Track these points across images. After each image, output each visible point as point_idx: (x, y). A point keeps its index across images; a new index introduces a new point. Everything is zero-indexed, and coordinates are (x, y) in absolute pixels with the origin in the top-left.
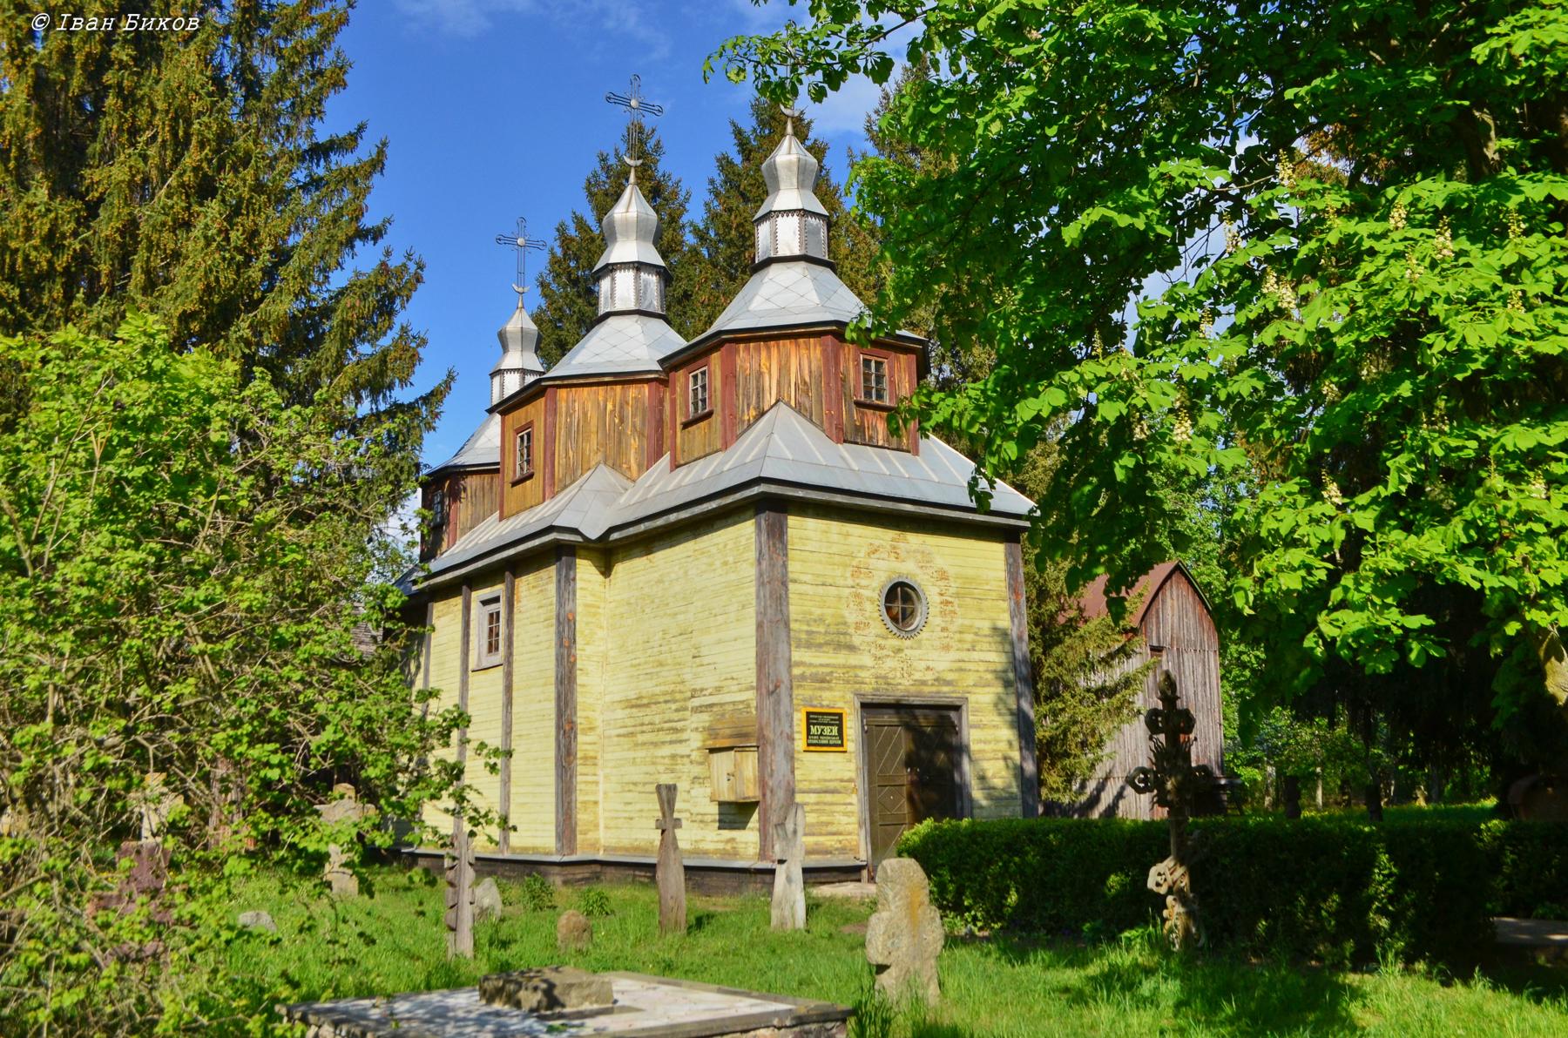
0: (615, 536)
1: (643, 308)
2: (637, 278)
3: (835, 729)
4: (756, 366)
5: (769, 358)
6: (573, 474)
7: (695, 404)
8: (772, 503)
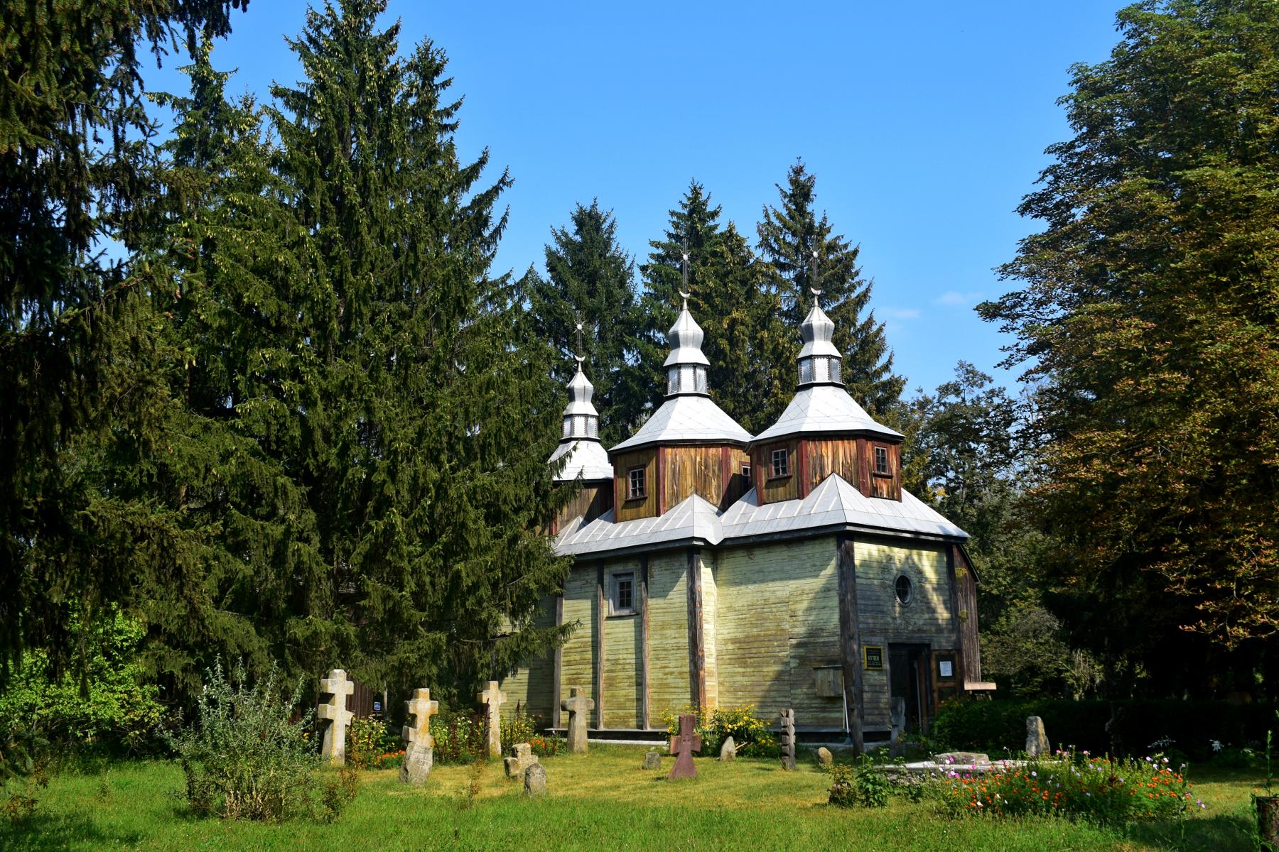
0: (728, 543)
6: (677, 498)
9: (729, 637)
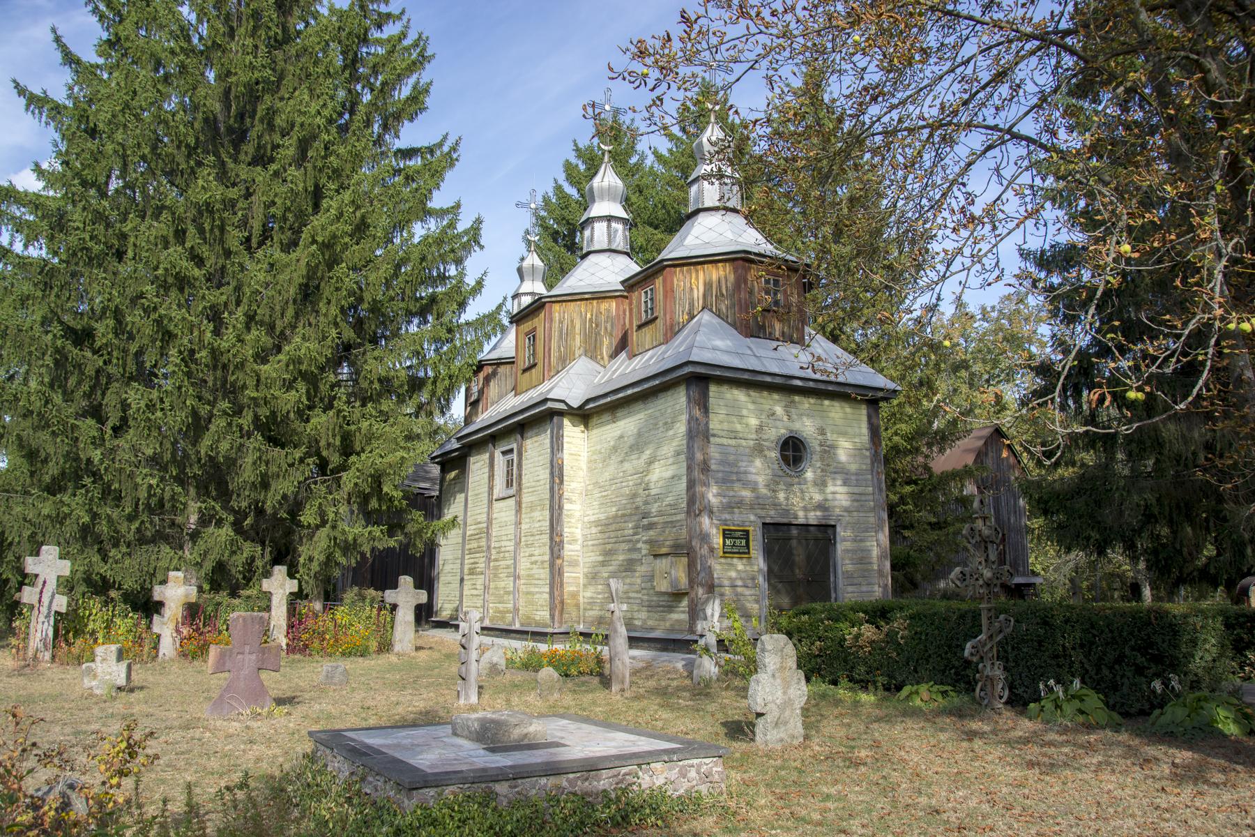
1: (613, 247)
2: (609, 227)
3: (744, 542)
4: (688, 285)
5: (697, 278)
6: (565, 360)
7: (646, 312)
8: (698, 380)
9: (592, 518)
